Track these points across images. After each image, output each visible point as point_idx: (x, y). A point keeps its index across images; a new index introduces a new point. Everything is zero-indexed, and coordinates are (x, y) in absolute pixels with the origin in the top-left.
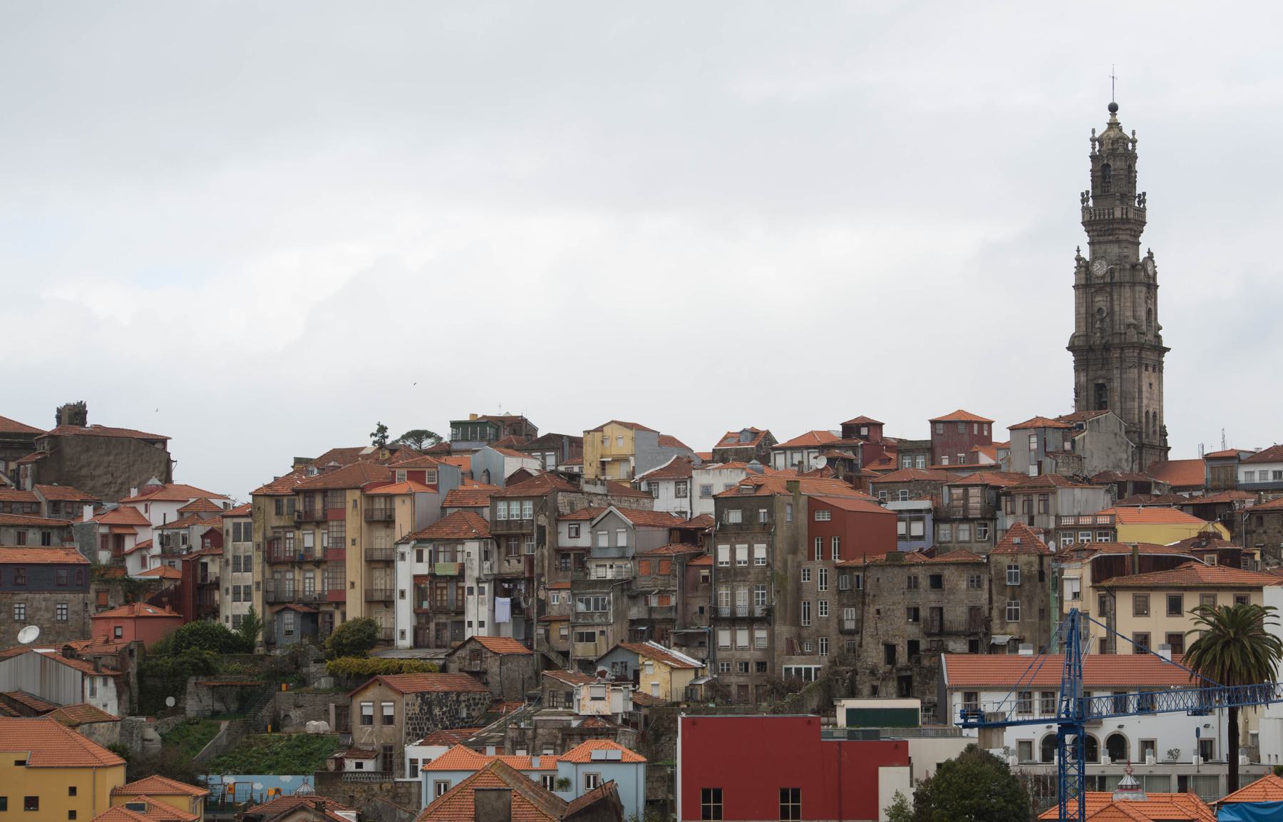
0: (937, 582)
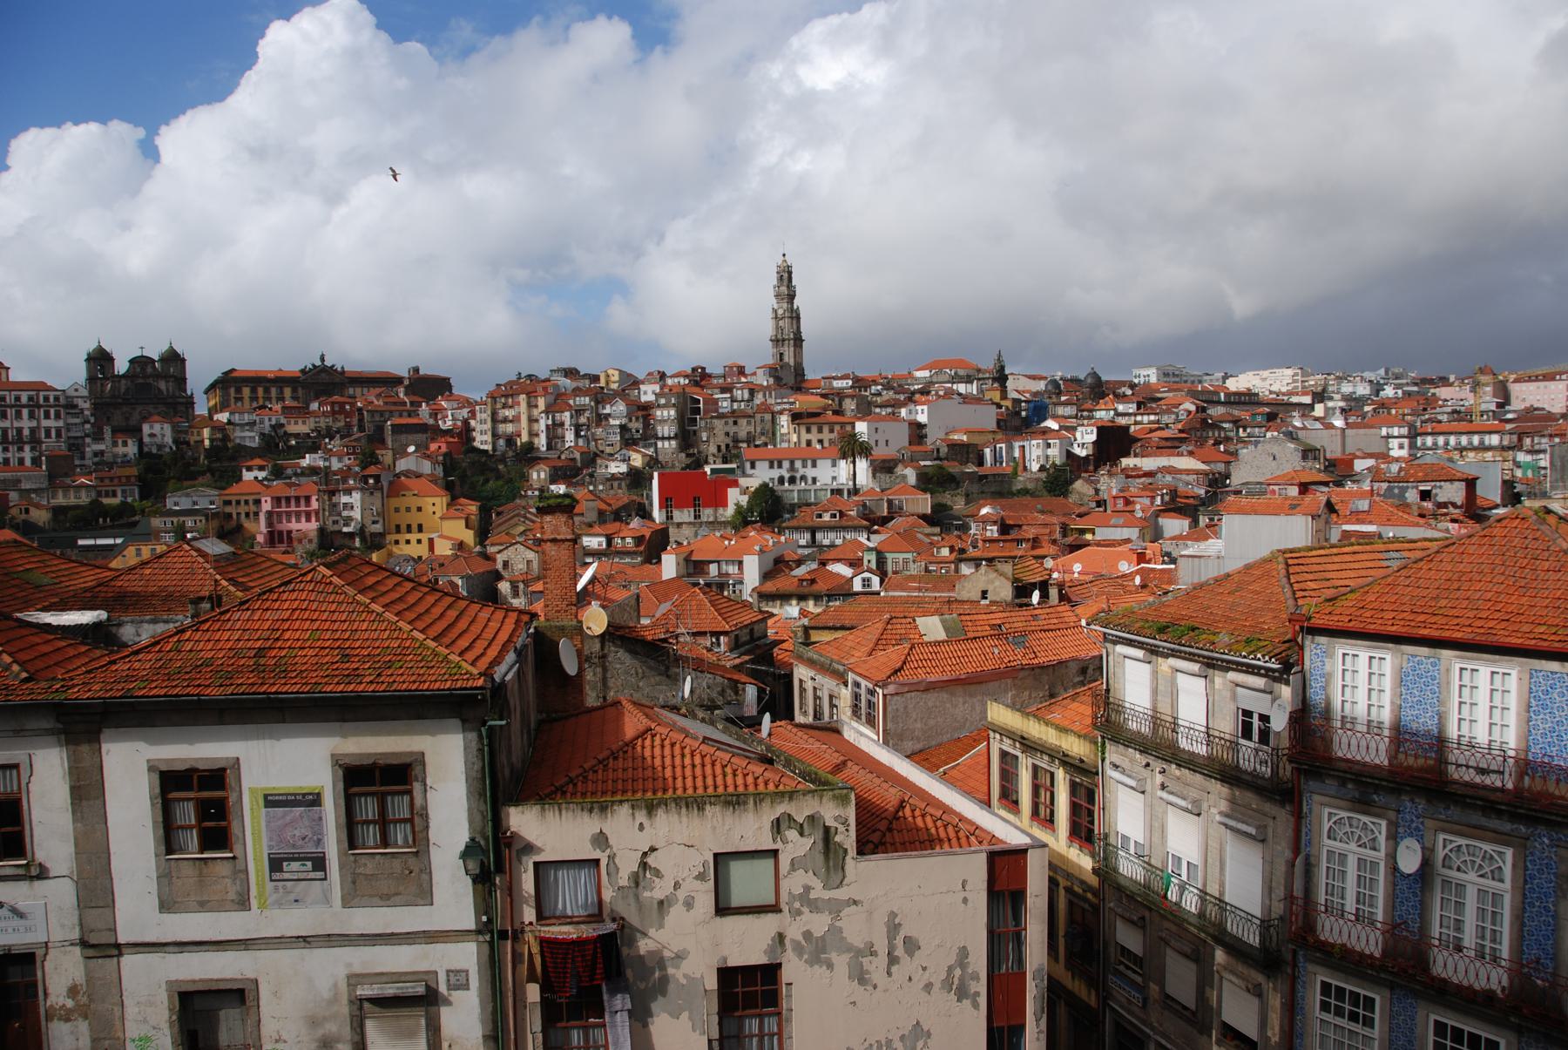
0: (735, 423)
